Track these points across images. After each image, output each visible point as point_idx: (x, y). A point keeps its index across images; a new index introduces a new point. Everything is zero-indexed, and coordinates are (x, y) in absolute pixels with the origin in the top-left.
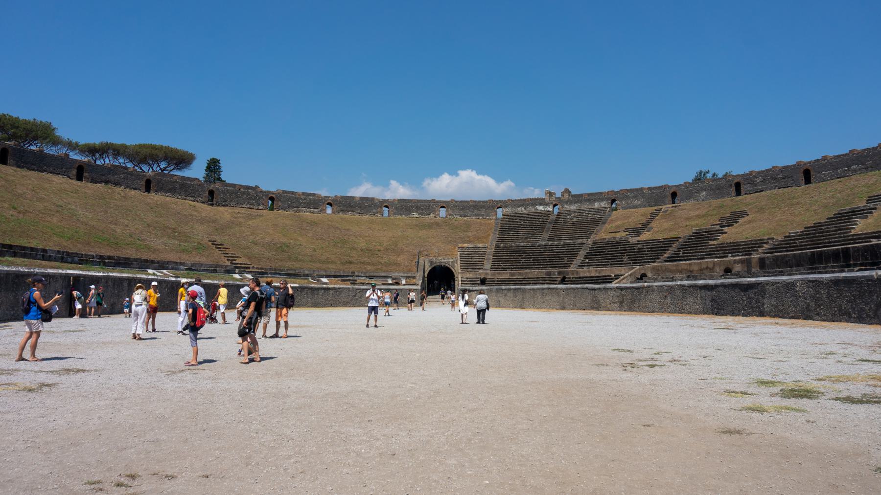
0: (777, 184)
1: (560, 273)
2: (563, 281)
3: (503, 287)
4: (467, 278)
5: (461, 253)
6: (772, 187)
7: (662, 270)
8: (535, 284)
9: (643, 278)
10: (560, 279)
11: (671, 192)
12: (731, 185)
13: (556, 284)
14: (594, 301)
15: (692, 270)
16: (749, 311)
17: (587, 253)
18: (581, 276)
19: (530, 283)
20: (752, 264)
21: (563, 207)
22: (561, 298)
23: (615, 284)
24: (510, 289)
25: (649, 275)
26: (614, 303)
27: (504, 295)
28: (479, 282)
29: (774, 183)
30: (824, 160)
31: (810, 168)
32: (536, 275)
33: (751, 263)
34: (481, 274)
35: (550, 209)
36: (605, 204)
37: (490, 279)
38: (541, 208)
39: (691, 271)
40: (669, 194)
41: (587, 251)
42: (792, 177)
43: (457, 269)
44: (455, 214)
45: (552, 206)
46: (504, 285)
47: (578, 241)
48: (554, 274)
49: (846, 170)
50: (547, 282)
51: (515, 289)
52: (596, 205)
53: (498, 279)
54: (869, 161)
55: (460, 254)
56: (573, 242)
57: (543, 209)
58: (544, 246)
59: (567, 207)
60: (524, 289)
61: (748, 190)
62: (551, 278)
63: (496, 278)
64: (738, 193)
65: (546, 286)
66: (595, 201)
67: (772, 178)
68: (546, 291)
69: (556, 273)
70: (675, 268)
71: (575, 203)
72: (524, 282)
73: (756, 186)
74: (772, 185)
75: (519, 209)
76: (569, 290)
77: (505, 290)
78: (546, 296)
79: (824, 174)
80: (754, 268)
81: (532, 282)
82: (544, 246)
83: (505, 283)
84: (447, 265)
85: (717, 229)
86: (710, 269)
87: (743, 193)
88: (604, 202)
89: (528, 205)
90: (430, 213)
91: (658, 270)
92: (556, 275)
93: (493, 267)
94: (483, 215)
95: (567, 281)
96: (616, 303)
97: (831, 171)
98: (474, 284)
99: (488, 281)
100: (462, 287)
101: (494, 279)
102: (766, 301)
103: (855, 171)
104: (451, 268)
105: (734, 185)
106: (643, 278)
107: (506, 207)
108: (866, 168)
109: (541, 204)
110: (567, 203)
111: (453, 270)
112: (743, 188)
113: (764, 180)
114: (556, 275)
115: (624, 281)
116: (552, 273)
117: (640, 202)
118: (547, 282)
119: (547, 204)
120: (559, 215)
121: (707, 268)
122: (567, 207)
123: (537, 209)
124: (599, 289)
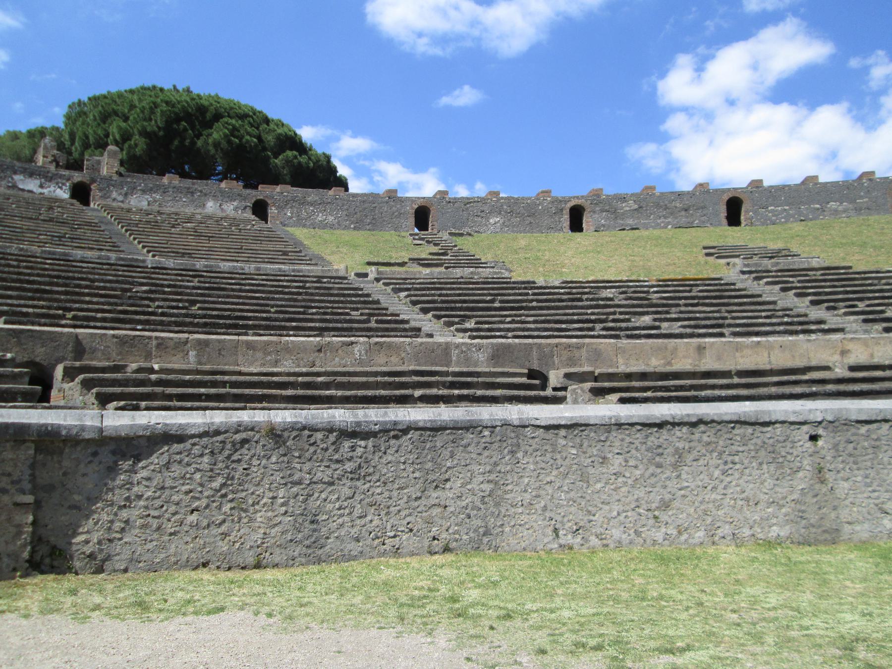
0: (670, 220)
6: (658, 224)
11: (416, 207)
12: (562, 210)
18: (622, 369)
22: (802, 479)
27: (356, 475)
29: (664, 216)
31: (741, 196)
32: (361, 363)
36: (236, 209)
38: (32, 185)
40: (410, 210)
42: (703, 208)
48: (467, 361)
49: (818, 209)
51: (436, 429)
52: (211, 206)
53: (139, 370)
54: (861, 197)
56: (294, 271)
60: (506, 424)
63: (134, 366)
64: (576, 225)
67: (658, 205)
68: (677, 438)
69: (482, 357)
71: (144, 192)
73: (623, 219)
74: (659, 221)
76: (864, 429)
78: (675, 466)
79: (772, 211)
81: (418, 393)
88: (235, 203)
103: (836, 212)
108: (858, 210)
109: (31, 174)
112: (587, 221)
113: (641, 207)
116: (455, 353)
117: (331, 218)
122: (120, 198)
123: (14, 187)
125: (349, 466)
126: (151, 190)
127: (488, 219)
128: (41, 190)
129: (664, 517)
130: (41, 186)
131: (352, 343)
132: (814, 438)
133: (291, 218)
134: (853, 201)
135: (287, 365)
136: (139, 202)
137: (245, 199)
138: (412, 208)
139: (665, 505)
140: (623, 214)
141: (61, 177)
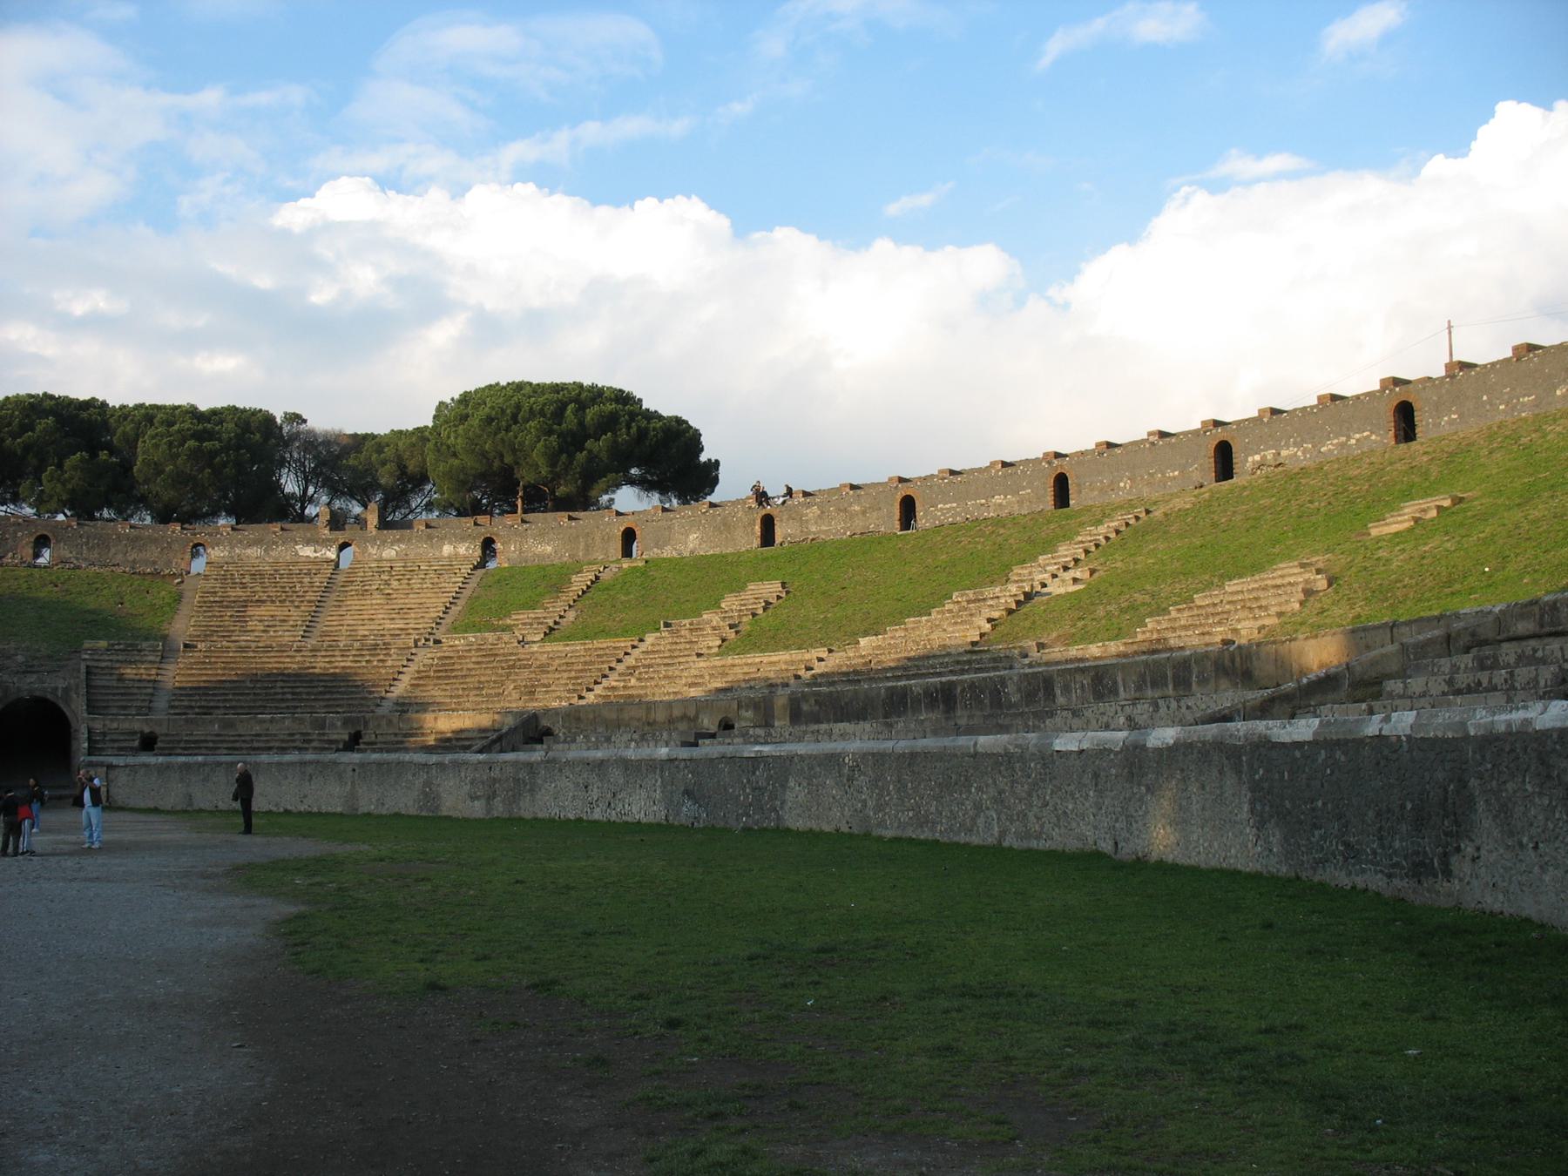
1: (346, 722)
2: (353, 743)
3: (200, 758)
4: (104, 734)
5: (89, 663)
7: (588, 719)
8: (283, 750)
9: (544, 738)
10: (346, 737)
11: (622, 529)
12: (754, 521)
13: (338, 750)
14: (426, 794)
15: (651, 721)
16: (757, 817)
17: (418, 672)
19: (270, 748)
20: (777, 711)
21: (365, 550)
23: (480, 751)
24: (219, 764)
25: (560, 732)
26: (474, 798)
28: (136, 743)
30: (944, 479)
33: (772, 708)
34: (139, 725)
35: (332, 555)
37: (167, 735)
39: (649, 724)
41: (416, 669)
43: (76, 710)
44: (77, 559)
45: (334, 549)
46: (204, 751)
47: (400, 643)
48: (333, 725)
49: (982, 505)
50: (315, 744)
52: (447, 549)
53: (187, 735)
55: (88, 667)
57: (313, 555)
58: (311, 651)
59: (374, 552)
60: (255, 762)
61: (790, 535)
62: (324, 734)
63: (184, 733)
65: (309, 757)
66: (442, 539)
68: (310, 770)
69: (339, 724)
70: (614, 716)
71: (392, 544)
72: (256, 745)
75: (249, 551)
77: (204, 764)
78: (310, 781)
80: (779, 719)
82: (311, 651)
83: (206, 748)
84: (49, 696)
85: (715, 623)
86: (689, 719)
87: (778, 539)
89: (275, 543)
90: (8, 552)
91: (578, 719)
92: (336, 728)
93: (176, 703)
94: (154, 563)
95: (364, 743)
96: (478, 798)
97: (955, 505)
98: (122, 751)
99: (161, 741)
100: (94, 759)
101: (177, 734)
102: (789, 796)
104: (62, 706)
105: (759, 522)
106: (544, 738)
107: (218, 545)
109: (308, 542)
110: (373, 541)
111: (68, 714)
113: (823, 512)
114: (336, 728)
115: (497, 746)
117: (549, 549)
118: (315, 744)
119: (325, 543)
120: (352, 571)
121: (684, 717)
123: (297, 554)
124: (440, 765)
125: (202, 777)
126: (399, 541)
127: (688, 536)
128: (315, 555)
129: (305, 801)
130: (315, 551)
131: (284, 718)
132: (354, 770)
133: (514, 551)
134: (1015, 493)
135: (257, 729)
136: (389, 553)
137: (474, 538)
138: (619, 530)
139: (305, 796)
140: (807, 521)
141: (329, 540)
